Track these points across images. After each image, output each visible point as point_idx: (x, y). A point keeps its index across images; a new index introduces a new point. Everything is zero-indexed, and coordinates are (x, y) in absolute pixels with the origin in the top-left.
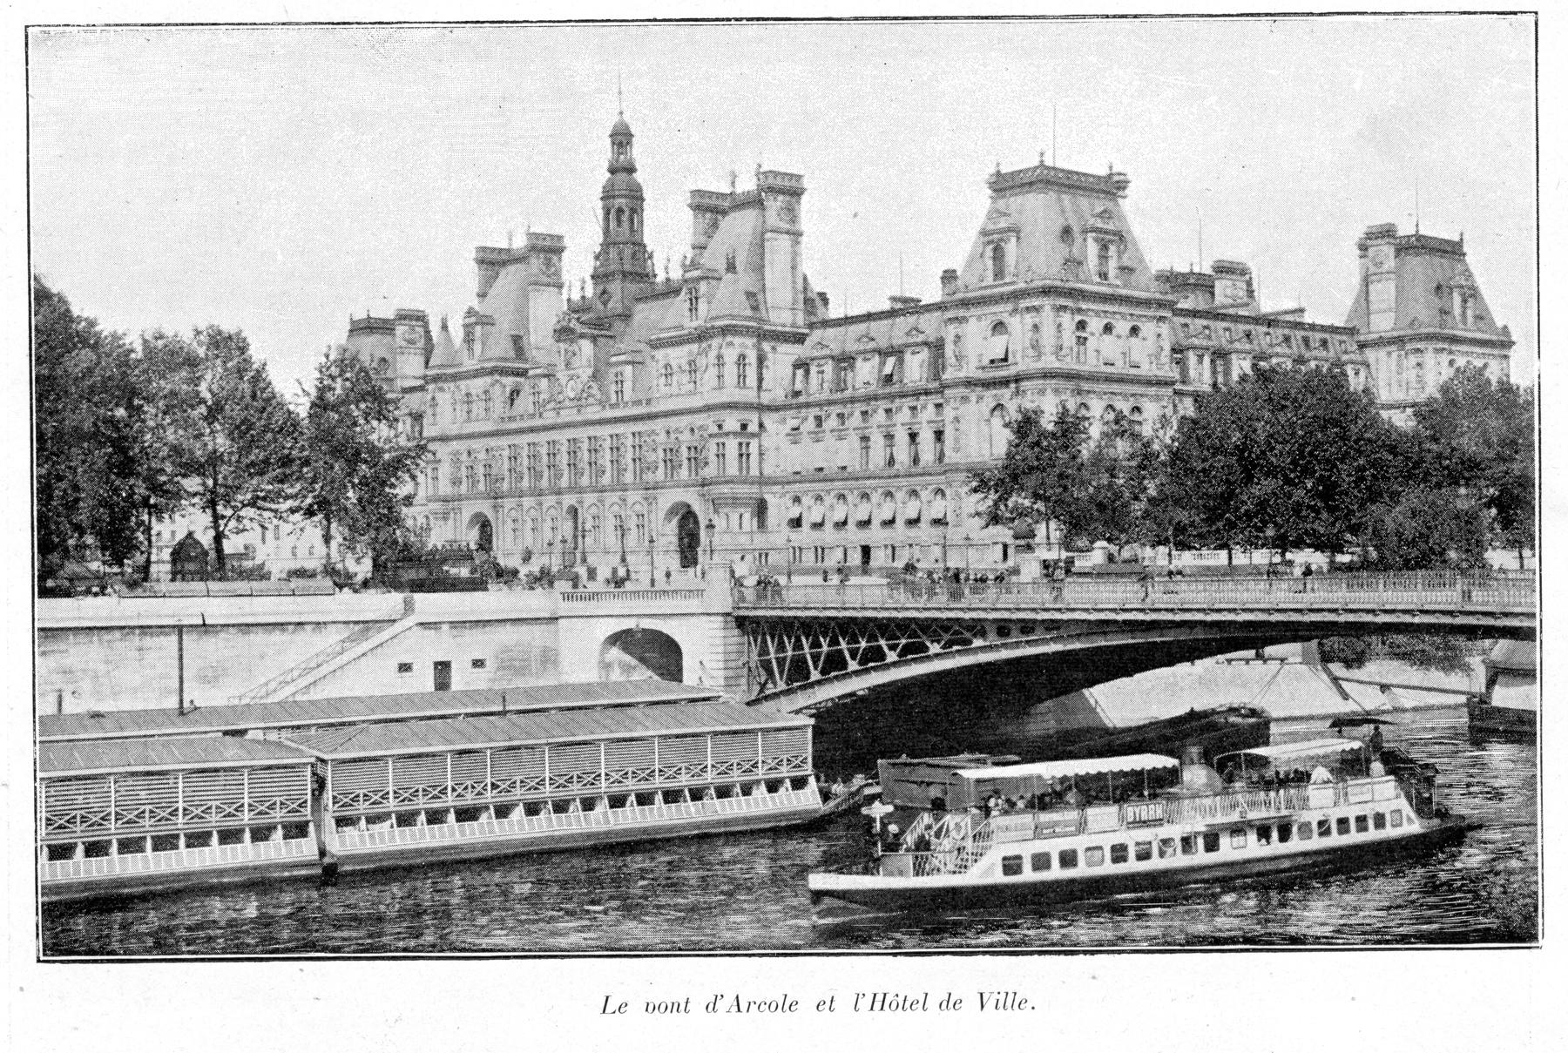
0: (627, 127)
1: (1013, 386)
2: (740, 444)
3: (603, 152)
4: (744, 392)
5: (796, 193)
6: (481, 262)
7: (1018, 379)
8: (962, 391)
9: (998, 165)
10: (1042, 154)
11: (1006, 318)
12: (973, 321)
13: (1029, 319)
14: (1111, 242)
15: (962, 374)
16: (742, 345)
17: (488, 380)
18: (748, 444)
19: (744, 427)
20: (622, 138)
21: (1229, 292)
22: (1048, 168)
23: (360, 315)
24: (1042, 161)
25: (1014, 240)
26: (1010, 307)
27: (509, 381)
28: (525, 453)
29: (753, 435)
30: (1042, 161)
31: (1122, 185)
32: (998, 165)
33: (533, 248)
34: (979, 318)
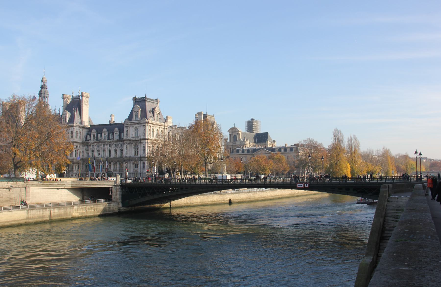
1: (139, 141)
2: (76, 150)
3: (40, 84)
4: (77, 139)
7: (140, 140)
8: (129, 142)
11: (138, 127)
12: (131, 127)
13: (144, 128)
14: (158, 113)
15: (128, 138)
16: (77, 129)
18: (77, 150)
19: (77, 147)
26: (139, 125)
29: (79, 149)
30: (145, 96)
34: (132, 127)
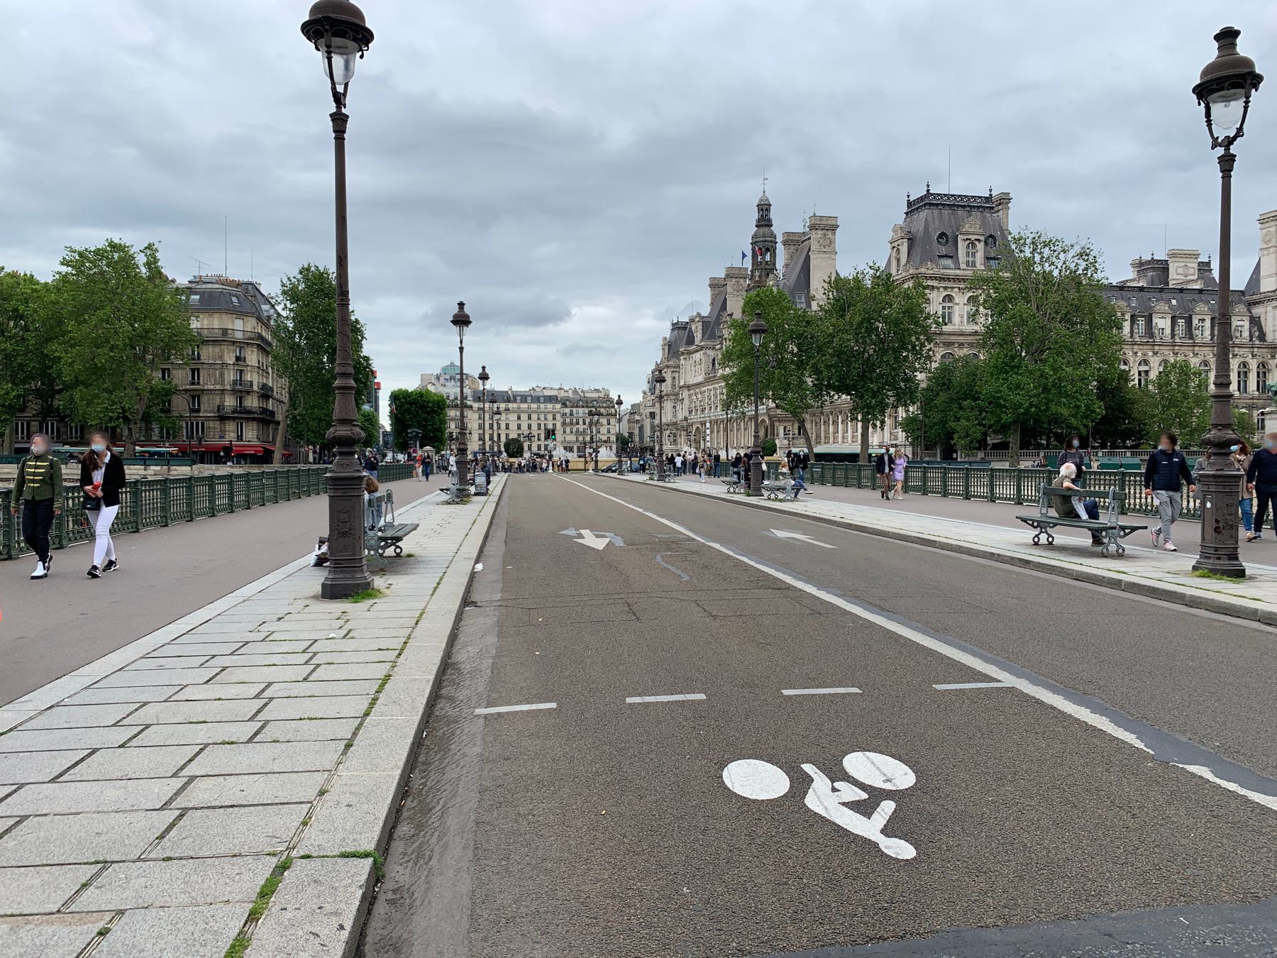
0: (767, 200)
5: (834, 228)
6: (711, 286)
9: (908, 196)
10: (928, 186)
17: (702, 352)
20: (764, 208)
21: (1180, 271)
22: (932, 194)
23: (675, 321)
24: (928, 191)
25: (906, 244)
27: (711, 353)
28: (712, 393)
30: (928, 191)
31: (1005, 200)
32: (908, 196)
33: (728, 276)
